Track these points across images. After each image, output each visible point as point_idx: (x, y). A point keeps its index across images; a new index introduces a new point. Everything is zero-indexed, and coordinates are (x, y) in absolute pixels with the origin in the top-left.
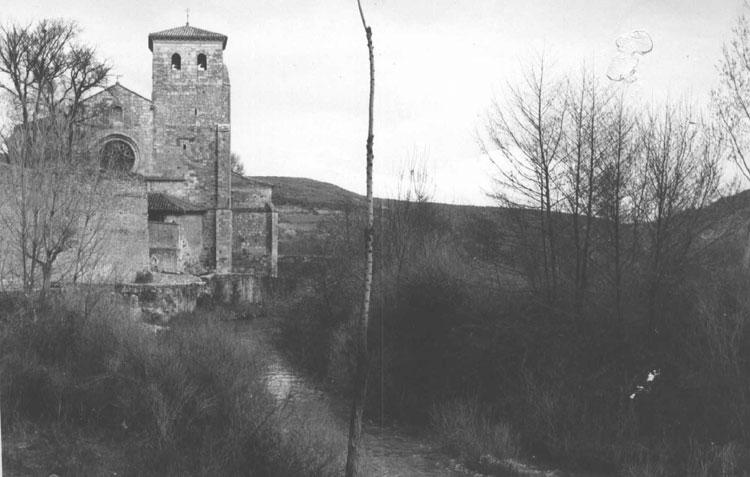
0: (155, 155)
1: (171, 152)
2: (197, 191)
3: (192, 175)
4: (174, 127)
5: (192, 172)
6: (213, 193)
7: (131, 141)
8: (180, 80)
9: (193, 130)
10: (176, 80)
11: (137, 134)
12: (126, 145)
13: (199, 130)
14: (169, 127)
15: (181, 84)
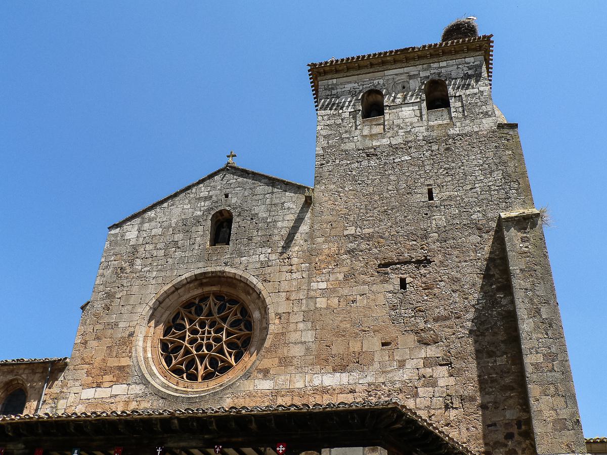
0: (313, 316)
1: (361, 302)
2: (453, 413)
3: (429, 362)
4: (370, 237)
5: (432, 351)
6: (511, 415)
7: (249, 288)
8: (382, 135)
9: (425, 237)
10: (372, 136)
11: (265, 265)
12: (234, 301)
13: (444, 236)
14: (355, 237)
15: (385, 141)
